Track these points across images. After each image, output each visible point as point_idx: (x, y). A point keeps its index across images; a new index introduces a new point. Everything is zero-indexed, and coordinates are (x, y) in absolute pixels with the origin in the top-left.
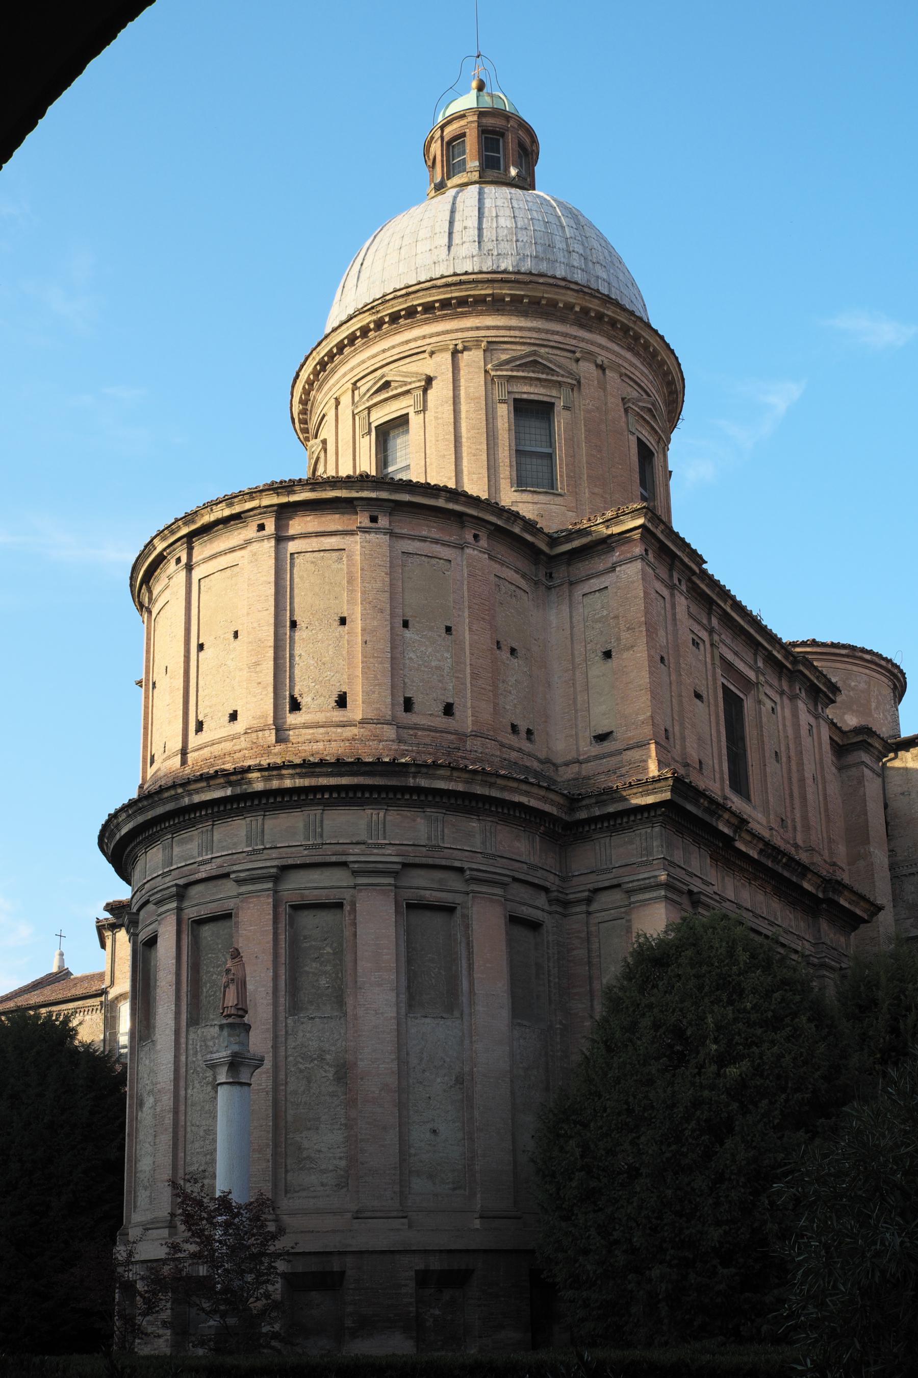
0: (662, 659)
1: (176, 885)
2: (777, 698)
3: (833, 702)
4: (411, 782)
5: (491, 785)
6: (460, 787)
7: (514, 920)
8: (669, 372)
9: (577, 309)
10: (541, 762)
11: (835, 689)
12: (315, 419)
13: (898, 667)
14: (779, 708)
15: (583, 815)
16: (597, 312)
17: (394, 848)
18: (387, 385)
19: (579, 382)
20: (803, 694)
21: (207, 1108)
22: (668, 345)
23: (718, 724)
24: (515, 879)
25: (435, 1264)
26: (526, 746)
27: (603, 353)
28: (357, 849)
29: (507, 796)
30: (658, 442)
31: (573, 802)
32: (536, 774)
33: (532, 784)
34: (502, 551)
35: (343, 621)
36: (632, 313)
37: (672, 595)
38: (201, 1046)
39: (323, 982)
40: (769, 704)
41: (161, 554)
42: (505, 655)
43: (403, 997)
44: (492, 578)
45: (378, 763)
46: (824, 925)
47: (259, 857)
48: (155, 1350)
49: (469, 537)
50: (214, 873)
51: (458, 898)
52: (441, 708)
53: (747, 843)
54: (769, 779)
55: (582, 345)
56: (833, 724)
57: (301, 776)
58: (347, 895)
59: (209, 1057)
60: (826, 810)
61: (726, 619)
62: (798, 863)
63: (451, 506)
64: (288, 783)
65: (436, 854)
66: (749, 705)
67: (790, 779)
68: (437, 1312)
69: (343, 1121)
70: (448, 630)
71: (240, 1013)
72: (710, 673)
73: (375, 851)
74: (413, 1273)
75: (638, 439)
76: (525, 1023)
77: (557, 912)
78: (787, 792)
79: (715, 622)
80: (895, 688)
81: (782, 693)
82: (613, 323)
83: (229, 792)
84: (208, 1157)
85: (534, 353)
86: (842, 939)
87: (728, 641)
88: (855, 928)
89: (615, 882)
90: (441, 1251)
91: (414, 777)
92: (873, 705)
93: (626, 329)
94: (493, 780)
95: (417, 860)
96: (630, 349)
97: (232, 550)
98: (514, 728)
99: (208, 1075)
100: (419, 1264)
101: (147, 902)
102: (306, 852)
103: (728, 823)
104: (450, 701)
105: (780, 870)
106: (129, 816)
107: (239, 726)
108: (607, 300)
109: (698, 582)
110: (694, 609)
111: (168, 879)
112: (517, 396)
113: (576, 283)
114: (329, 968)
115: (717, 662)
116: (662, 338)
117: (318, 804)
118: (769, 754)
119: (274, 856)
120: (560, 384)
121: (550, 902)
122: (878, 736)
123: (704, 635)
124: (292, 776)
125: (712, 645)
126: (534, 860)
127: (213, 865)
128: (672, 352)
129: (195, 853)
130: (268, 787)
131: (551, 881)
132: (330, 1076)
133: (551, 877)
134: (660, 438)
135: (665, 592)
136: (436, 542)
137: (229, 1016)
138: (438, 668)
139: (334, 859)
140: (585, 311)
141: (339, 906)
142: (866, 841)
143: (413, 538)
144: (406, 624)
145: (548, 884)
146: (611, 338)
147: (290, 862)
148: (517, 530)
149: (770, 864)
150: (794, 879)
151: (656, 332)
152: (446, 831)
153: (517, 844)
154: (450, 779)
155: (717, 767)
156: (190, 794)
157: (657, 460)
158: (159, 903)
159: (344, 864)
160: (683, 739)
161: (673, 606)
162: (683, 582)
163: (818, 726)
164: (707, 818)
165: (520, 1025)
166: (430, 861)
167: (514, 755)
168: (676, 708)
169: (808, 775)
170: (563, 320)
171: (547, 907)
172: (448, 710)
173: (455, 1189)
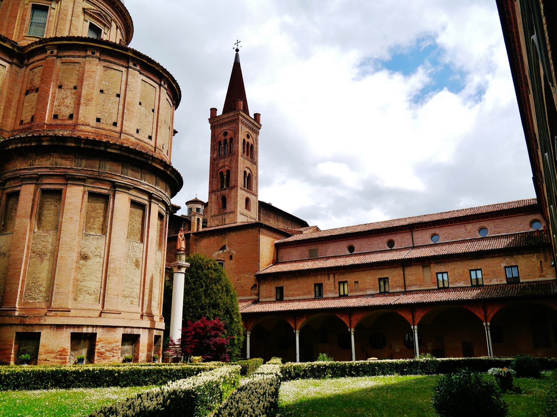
21: (132, 271)
48: (111, 361)
84: (132, 290)
99: (134, 259)
111: (125, 180)
127: (147, 187)
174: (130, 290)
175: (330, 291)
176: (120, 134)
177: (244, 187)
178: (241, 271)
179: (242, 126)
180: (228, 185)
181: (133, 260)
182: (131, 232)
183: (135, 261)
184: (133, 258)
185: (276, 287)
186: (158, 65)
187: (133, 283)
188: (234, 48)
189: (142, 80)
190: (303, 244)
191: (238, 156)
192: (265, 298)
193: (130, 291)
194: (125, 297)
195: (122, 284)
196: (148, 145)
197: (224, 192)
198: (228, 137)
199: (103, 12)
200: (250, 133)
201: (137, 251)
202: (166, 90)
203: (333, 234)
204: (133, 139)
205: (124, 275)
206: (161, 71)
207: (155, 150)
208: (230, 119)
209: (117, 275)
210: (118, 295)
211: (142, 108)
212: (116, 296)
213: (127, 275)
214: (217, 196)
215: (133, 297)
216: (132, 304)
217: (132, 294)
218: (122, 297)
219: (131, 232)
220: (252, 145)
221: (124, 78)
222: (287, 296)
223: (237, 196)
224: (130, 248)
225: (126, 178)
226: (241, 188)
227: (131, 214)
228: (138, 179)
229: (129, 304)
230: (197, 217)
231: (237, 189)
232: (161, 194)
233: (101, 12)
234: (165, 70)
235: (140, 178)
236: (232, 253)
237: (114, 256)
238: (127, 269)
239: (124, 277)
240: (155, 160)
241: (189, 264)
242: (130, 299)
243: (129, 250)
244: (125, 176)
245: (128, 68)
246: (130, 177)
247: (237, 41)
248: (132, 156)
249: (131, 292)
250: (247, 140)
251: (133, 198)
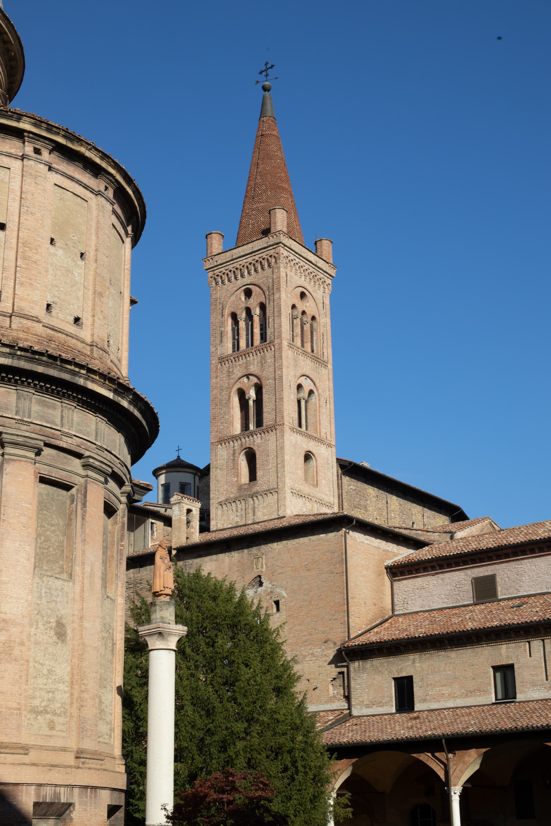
21: (50, 650)
38: (46, 592)
50: (73, 448)
84: (50, 694)
99: (52, 620)
111: (25, 428)
119: (108, 458)
156: (87, 379)
174: (47, 696)
175: (534, 684)
176: (10, 317)
177: (300, 426)
178: (304, 639)
179: (289, 273)
180: (259, 423)
181: (50, 622)
182: (43, 553)
183: (54, 625)
184: (50, 616)
185: (395, 679)
187: (53, 677)
188: (258, 82)
189: (55, 184)
190: (457, 564)
191: (280, 348)
192: (368, 706)
193: (46, 699)
194: (36, 712)
195: (27, 681)
196: (74, 341)
197: (248, 442)
198: (254, 303)
200: (308, 288)
201: (58, 599)
202: (112, 204)
203: (534, 537)
204: (38, 328)
205: (31, 660)
207: (92, 350)
208: (257, 258)
209: (16, 660)
210: (19, 709)
211: (58, 251)
212: (15, 712)
213: (37, 659)
214: (231, 452)
215: (54, 713)
216: (52, 728)
217: (52, 706)
218: (29, 712)
219: (43, 553)
220: (313, 318)
221: (16, 186)
222: (424, 701)
223: (282, 448)
224: (43, 592)
225: (26, 422)
226: (292, 429)
227: (42, 509)
228: (55, 424)
229: (46, 731)
230: (186, 507)
231: (283, 431)
232: (109, 457)
235: (58, 421)
236: (279, 595)
237: (6, 613)
238: (37, 643)
239: (31, 664)
241: (186, 628)
242: (48, 716)
243: (40, 597)
244: (25, 419)
245: (23, 158)
246: (37, 419)
247: (266, 64)
248: (40, 369)
249: (49, 700)
250: (301, 307)
251: (46, 471)
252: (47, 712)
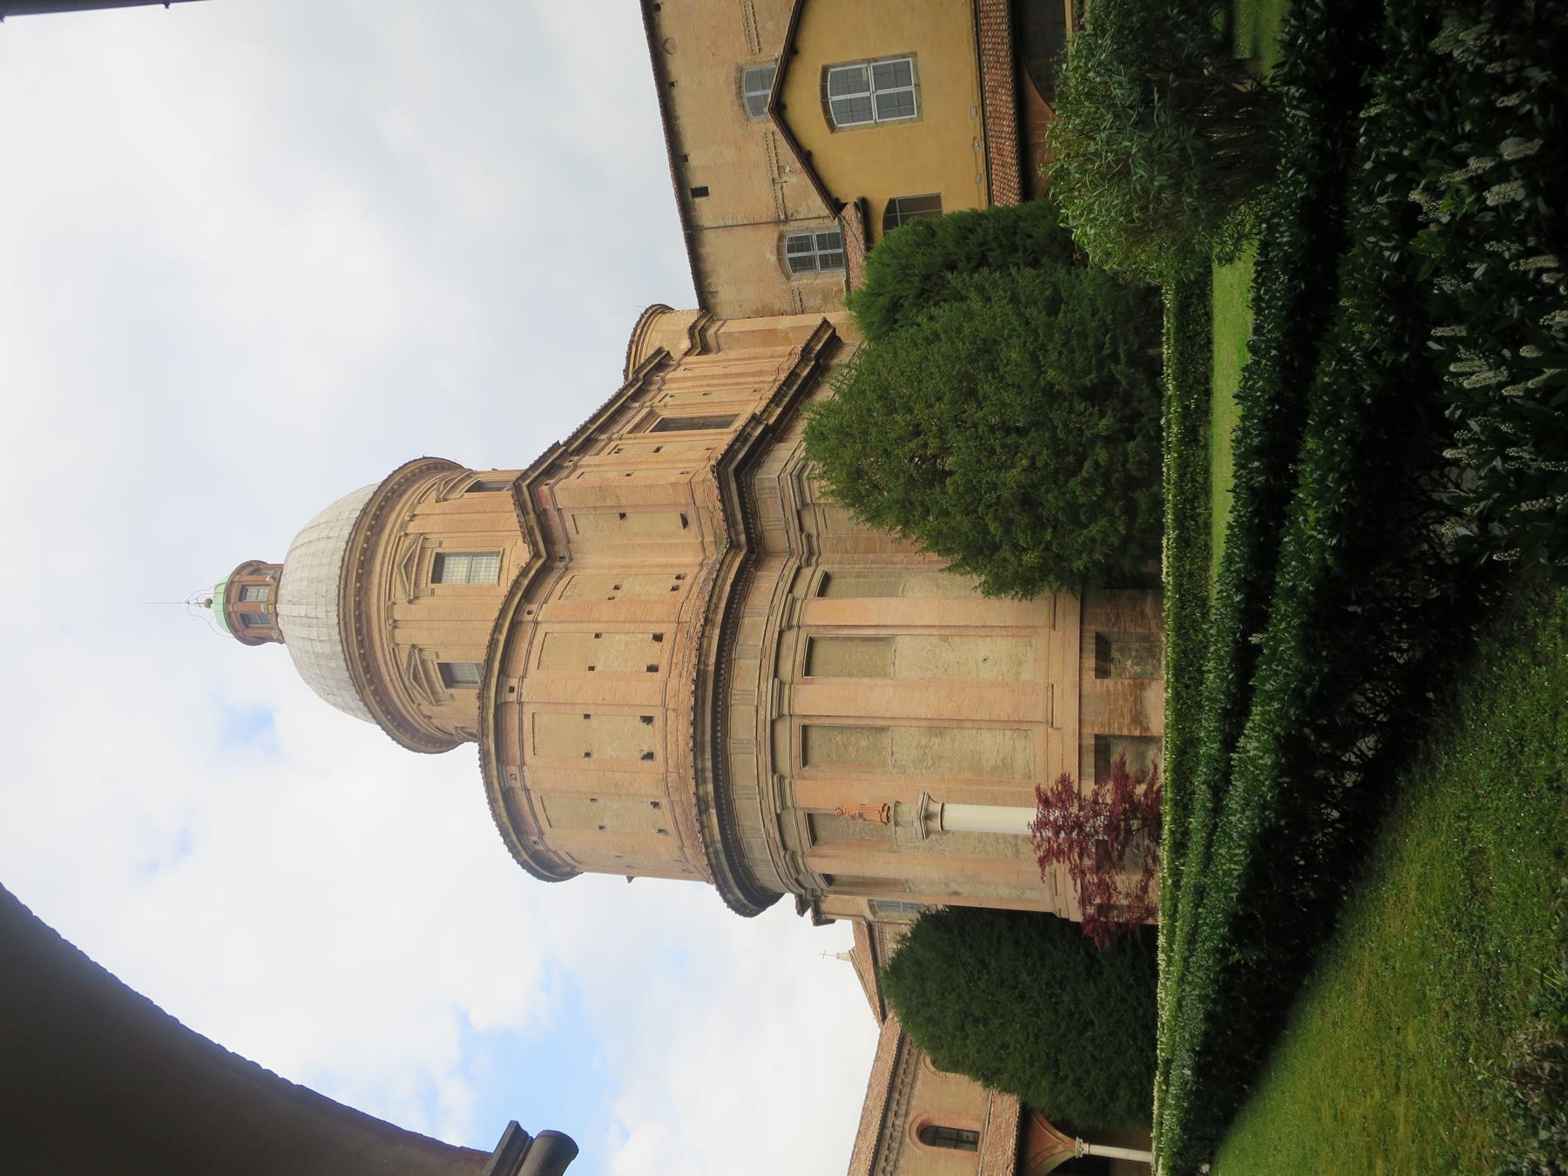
0: (628, 475)
1: (784, 857)
2: (662, 394)
3: (668, 352)
4: (711, 668)
5: (717, 607)
6: (717, 631)
7: (822, 592)
8: (420, 469)
9: (369, 533)
10: (700, 571)
11: (660, 351)
12: (439, 734)
13: (647, 310)
14: (671, 392)
15: (743, 537)
16: (372, 519)
17: (761, 685)
18: (415, 678)
19: (422, 534)
20: (662, 374)
22: (400, 468)
23: (680, 436)
24: (791, 591)
25: (1091, 662)
26: (689, 580)
27: (402, 516)
28: (761, 712)
29: (725, 595)
30: (470, 477)
31: (733, 546)
32: (709, 573)
33: (717, 576)
34: (542, 593)
35: (587, 716)
36: (375, 493)
37: (581, 467)
39: (864, 743)
40: (667, 399)
41: (530, 856)
42: (619, 594)
43: (878, 681)
44: (561, 602)
45: (695, 693)
46: (835, 361)
47: (765, 789)
49: (530, 618)
50: (776, 826)
51: (803, 635)
52: (656, 643)
53: (770, 415)
54: (723, 400)
55: (395, 531)
56: (686, 354)
57: (703, 752)
58: (797, 722)
59: (920, 836)
60: (749, 359)
61: (602, 429)
62: (788, 379)
63: (505, 631)
64: (709, 764)
65: (768, 651)
66: (666, 414)
67: (724, 385)
68: (1129, 663)
69: (975, 731)
70: (597, 636)
71: (886, 809)
72: (641, 441)
73: (763, 698)
74: (1098, 681)
75: (467, 491)
76: (901, 588)
77: (817, 561)
78: (734, 387)
79: (604, 437)
80: (663, 312)
81: (660, 390)
82: (381, 508)
83: (713, 811)
85: (399, 566)
86: (847, 348)
87: (618, 427)
88: (839, 339)
89: (795, 515)
90: (1081, 658)
91: (708, 665)
92: (675, 328)
93: (386, 499)
94: (713, 605)
95: (772, 666)
96: (401, 496)
97: (530, 800)
98: (674, 589)
100: (1090, 675)
101: (797, 880)
102: (762, 753)
103: (754, 429)
104: (651, 636)
105: (792, 392)
106: (729, 892)
107: (664, 802)
108: (364, 511)
109: (572, 448)
110: (594, 451)
111: (780, 864)
112: (430, 580)
113: (351, 534)
114: (853, 739)
115: (632, 435)
116: (395, 472)
117: (725, 742)
118: (705, 399)
120: (423, 549)
121: (809, 565)
122: (696, 321)
123: (612, 445)
124: (703, 760)
125: (620, 439)
126: (775, 576)
127: (769, 826)
128: (405, 465)
129: (760, 840)
130: (711, 780)
131: (793, 564)
132: (938, 740)
133: (790, 564)
134: (467, 476)
135: (579, 472)
136: (531, 643)
137: (888, 818)
138: (626, 645)
139: (768, 731)
140: (371, 528)
141: (805, 728)
142: (773, 332)
143: (527, 661)
144: (592, 668)
145: (795, 567)
146: (392, 509)
147: (769, 765)
148: (526, 582)
149: (787, 400)
150: (799, 382)
151: (390, 476)
152: (750, 643)
153: (763, 589)
154: (710, 638)
155: (712, 437)
156: (714, 842)
157: (482, 479)
158: (798, 871)
159: (773, 722)
160: (688, 461)
161: (589, 466)
162: (572, 458)
163: (686, 364)
164: (749, 443)
165: (903, 591)
166: (773, 656)
167: (695, 590)
168: (664, 465)
169: (722, 371)
170: (376, 544)
171: (812, 568)
172: (658, 638)
173: (1031, 646)
186: (496, 816)
196: (681, 829)
199: (406, 679)
206: (501, 803)
211: (606, 822)
233: (409, 679)
234: (510, 850)
240: (708, 840)
242: (1019, 843)
252: (1016, 844)
